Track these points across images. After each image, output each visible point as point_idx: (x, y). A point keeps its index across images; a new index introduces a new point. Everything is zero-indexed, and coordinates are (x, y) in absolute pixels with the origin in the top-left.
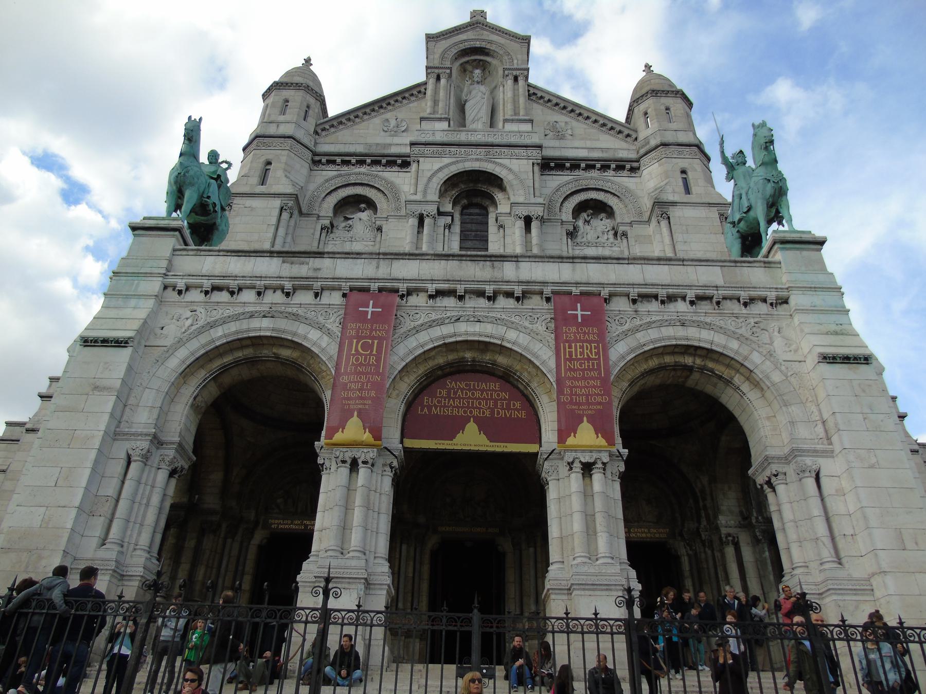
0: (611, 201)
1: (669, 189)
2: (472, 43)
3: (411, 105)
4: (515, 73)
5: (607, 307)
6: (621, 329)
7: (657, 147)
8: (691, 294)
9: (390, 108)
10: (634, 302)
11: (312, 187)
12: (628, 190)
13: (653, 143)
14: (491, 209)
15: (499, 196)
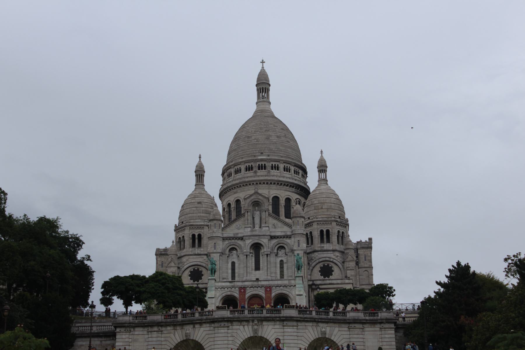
0: (285, 246)
1: (295, 246)
2: (255, 199)
3: (242, 219)
4: (265, 210)
5: (272, 288)
6: (274, 291)
7: (294, 234)
8: (283, 286)
9: (237, 221)
10: (276, 287)
11: (224, 246)
12: (288, 243)
13: (294, 233)
14: (260, 250)
15: (262, 248)
